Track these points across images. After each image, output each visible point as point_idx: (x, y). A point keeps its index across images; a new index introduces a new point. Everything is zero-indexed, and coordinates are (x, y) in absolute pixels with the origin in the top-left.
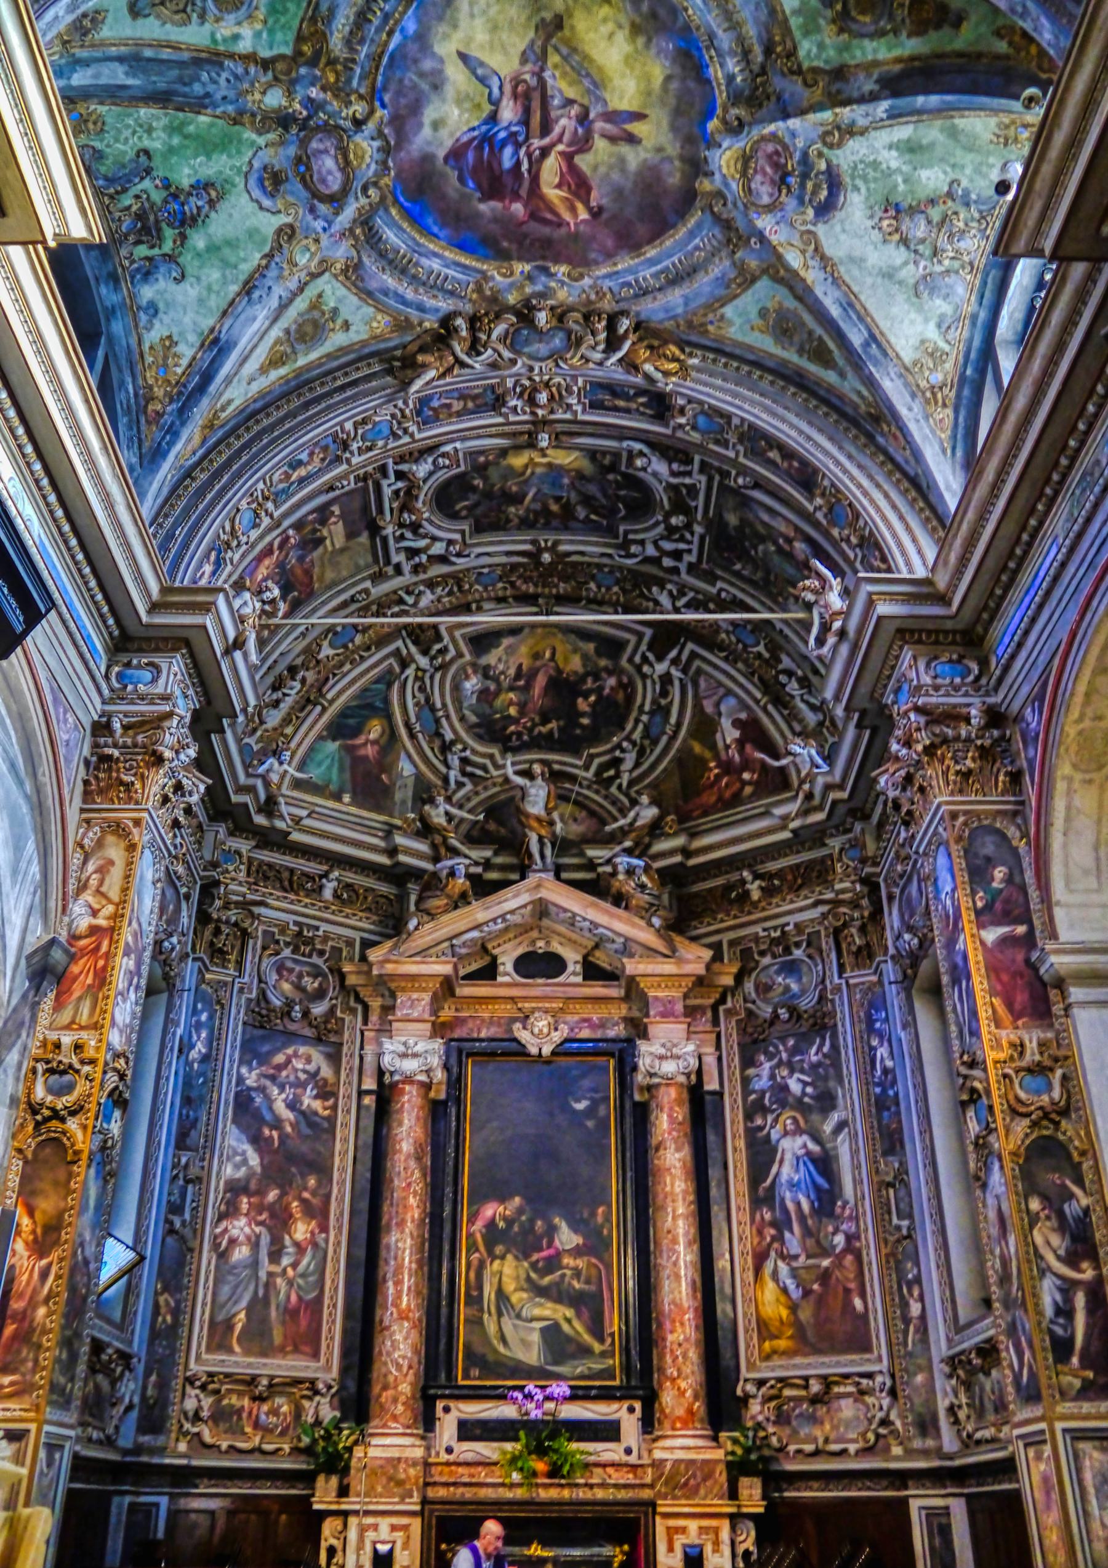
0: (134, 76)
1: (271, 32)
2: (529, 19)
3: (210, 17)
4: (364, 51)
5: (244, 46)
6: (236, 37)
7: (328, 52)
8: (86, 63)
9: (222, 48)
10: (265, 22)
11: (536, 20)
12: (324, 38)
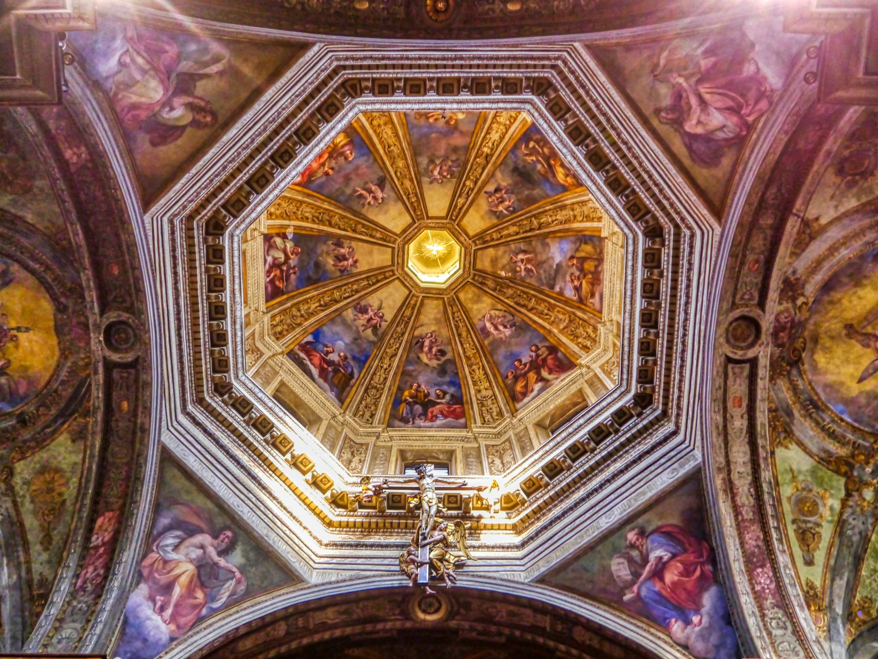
0: (843, 574)
1: (832, 487)
2: (844, 342)
3: (819, 521)
4: (850, 436)
5: (837, 505)
6: (832, 508)
7: (847, 457)
8: (831, 601)
9: (836, 518)
10: (826, 490)
11: (846, 339)
12: (839, 459)
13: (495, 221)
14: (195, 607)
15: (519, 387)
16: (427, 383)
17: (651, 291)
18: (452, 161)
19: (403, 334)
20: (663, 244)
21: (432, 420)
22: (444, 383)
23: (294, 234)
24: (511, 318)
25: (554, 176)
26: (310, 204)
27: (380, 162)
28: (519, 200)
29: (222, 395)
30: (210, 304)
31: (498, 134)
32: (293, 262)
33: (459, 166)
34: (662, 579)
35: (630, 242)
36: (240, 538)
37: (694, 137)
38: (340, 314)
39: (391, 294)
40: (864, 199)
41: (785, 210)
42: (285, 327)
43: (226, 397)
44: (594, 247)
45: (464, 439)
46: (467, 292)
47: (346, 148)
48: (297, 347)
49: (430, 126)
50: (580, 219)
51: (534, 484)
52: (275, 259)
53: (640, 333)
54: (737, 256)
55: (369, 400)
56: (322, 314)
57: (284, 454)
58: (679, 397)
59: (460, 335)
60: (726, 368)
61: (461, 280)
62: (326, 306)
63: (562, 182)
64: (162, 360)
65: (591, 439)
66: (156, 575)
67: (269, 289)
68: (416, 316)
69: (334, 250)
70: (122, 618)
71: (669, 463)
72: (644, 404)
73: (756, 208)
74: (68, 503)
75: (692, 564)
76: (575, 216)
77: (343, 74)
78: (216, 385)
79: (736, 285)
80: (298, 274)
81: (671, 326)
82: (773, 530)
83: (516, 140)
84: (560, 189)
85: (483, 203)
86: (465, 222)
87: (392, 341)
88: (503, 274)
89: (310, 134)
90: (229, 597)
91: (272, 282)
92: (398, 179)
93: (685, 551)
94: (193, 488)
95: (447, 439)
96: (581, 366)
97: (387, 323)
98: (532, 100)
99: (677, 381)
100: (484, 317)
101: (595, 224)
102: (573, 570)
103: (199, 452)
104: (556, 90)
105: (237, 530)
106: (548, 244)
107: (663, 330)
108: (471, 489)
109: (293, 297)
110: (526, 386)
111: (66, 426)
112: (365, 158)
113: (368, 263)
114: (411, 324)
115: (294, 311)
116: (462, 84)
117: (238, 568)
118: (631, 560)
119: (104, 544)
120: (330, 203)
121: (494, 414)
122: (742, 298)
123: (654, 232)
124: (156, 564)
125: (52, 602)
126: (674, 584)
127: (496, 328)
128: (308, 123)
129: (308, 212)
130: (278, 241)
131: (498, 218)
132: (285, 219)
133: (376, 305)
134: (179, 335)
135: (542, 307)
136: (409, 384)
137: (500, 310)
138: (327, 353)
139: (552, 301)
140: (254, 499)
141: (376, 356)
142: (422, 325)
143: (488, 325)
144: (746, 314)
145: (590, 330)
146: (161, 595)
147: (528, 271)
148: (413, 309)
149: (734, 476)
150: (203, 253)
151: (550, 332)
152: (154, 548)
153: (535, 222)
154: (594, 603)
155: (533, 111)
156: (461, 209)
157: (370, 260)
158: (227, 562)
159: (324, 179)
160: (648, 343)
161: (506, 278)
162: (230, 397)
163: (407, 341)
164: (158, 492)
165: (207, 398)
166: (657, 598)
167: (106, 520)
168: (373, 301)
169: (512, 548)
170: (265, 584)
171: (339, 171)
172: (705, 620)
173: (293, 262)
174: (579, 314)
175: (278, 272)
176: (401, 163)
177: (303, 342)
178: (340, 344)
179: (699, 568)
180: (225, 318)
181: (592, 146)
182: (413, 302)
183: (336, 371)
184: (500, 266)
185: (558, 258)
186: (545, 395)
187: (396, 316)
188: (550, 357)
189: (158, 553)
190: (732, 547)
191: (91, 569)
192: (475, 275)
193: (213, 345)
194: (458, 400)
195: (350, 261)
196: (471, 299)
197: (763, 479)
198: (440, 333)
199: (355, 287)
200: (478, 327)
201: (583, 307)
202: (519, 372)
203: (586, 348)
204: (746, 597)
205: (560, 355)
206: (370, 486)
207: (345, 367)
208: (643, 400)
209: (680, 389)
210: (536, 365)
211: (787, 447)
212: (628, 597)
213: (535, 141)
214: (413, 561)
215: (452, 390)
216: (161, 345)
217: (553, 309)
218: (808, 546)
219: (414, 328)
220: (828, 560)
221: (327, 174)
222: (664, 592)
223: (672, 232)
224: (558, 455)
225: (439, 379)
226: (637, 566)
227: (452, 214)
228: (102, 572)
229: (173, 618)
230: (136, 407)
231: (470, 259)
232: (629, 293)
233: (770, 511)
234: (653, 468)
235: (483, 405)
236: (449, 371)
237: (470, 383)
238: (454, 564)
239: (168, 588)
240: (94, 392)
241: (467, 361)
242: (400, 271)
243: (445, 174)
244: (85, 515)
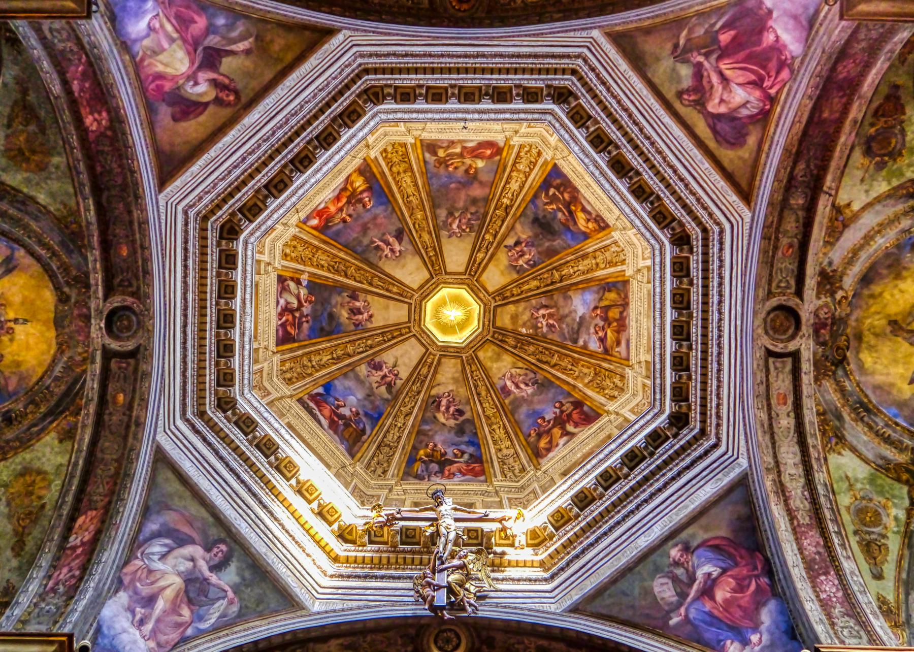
1: (894, 496)
2: (890, 340)
3: (884, 532)
5: (902, 515)
6: (896, 519)
7: (907, 464)
9: (902, 529)
10: (888, 499)
11: (891, 336)
12: (898, 465)
13: (515, 276)
14: (178, 625)
15: (543, 444)
16: (444, 442)
17: (681, 301)
18: (471, 214)
19: (419, 393)
20: (691, 251)
21: (448, 477)
22: (462, 443)
24: (532, 375)
25: (575, 223)
26: (326, 251)
27: (399, 213)
28: (539, 253)
29: (224, 411)
30: (219, 311)
31: (518, 184)
32: (306, 309)
33: (478, 219)
34: (712, 598)
35: (657, 253)
36: (236, 554)
37: (718, 117)
39: (406, 352)
40: (895, 183)
41: (815, 188)
42: (295, 375)
43: (229, 413)
44: (619, 294)
45: (484, 493)
46: (487, 351)
47: (365, 195)
48: (306, 396)
49: (450, 176)
50: (603, 266)
51: (563, 517)
52: (288, 303)
53: (671, 346)
54: (770, 239)
55: (381, 457)
56: (334, 367)
57: (288, 480)
58: (718, 405)
59: (479, 394)
60: (767, 362)
61: (480, 338)
63: (583, 229)
64: (164, 352)
65: (623, 464)
66: (138, 585)
67: (280, 333)
68: (433, 375)
69: (349, 302)
70: (95, 625)
71: (712, 475)
72: (680, 425)
73: (786, 186)
74: (48, 507)
75: (744, 579)
76: (597, 264)
77: (366, 80)
78: (219, 399)
79: (771, 271)
80: (311, 323)
81: (705, 336)
82: (833, 535)
83: (535, 189)
84: (582, 238)
85: (503, 258)
86: (484, 277)
87: (406, 400)
88: (524, 331)
89: (330, 139)
90: (220, 617)
91: (283, 325)
92: (417, 231)
93: (737, 564)
94: (188, 494)
95: (466, 492)
96: (608, 412)
98: (553, 110)
99: (714, 387)
100: (504, 376)
101: (619, 268)
102: (610, 595)
103: (197, 459)
104: (577, 98)
105: (233, 544)
107: (697, 341)
108: (493, 520)
109: (305, 346)
110: (550, 442)
111: (54, 425)
114: (427, 382)
115: (305, 361)
116: (483, 92)
117: (231, 588)
118: (675, 579)
119: (83, 544)
120: (347, 253)
121: (517, 471)
122: (778, 287)
123: (681, 240)
124: (139, 572)
125: (17, 603)
126: (726, 601)
127: (517, 387)
128: (330, 129)
129: (323, 259)
130: (292, 285)
131: (518, 272)
134: (184, 333)
135: (565, 363)
136: (424, 444)
138: (338, 407)
139: (576, 355)
140: (253, 516)
141: (389, 414)
143: (509, 383)
144: (784, 303)
145: (617, 380)
146: (143, 607)
147: (550, 326)
148: (430, 367)
149: (786, 479)
150: (216, 257)
151: (574, 387)
152: (139, 555)
153: (557, 275)
154: (636, 631)
155: (554, 121)
156: (480, 264)
158: (220, 579)
160: (681, 358)
161: (527, 335)
162: (234, 414)
163: (423, 400)
164: (148, 495)
165: (209, 412)
166: (708, 619)
167: (88, 520)
168: (388, 358)
169: (540, 581)
170: (261, 608)
171: (356, 220)
172: (765, 638)
173: (306, 309)
175: (290, 317)
176: (419, 215)
178: (352, 399)
179: (754, 583)
180: (235, 269)
181: (615, 153)
182: (429, 360)
183: (347, 425)
184: (520, 322)
186: (571, 445)
187: (411, 375)
188: (575, 412)
189: (143, 560)
190: (790, 553)
191: (65, 570)
192: (494, 333)
193: (219, 356)
194: (477, 459)
195: (365, 315)
196: (490, 358)
197: (817, 481)
199: (369, 342)
200: (498, 386)
201: (609, 358)
202: (542, 429)
203: (623, 262)
204: (811, 604)
205: (585, 408)
206: (383, 514)
207: (357, 422)
208: (679, 420)
209: (718, 396)
210: (560, 421)
211: (839, 453)
212: (674, 621)
213: (555, 188)
214: (429, 584)
215: (471, 450)
216: (165, 336)
217: (577, 363)
218: (875, 558)
219: (431, 387)
220: (899, 573)
221: (344, 221)
222: (716, 613)
223: (700, 237)
224: (588, 483)
225: (457, 439)
226: (682, 586)
228: (77, 573)
229: (154, 632)
230: (133, 399)
231: (490, 314)
232: (658, 306)
233: (828, 514)
234: (694, 482)
235: (504, 464)
236: (467, 431)
237: (490, 442)
238: (475, 594)
239: (150, 601)
240: (89, 384)
241: (486, 420)
242: (417, 328)
243: (464, 227)
244: (65, 513)
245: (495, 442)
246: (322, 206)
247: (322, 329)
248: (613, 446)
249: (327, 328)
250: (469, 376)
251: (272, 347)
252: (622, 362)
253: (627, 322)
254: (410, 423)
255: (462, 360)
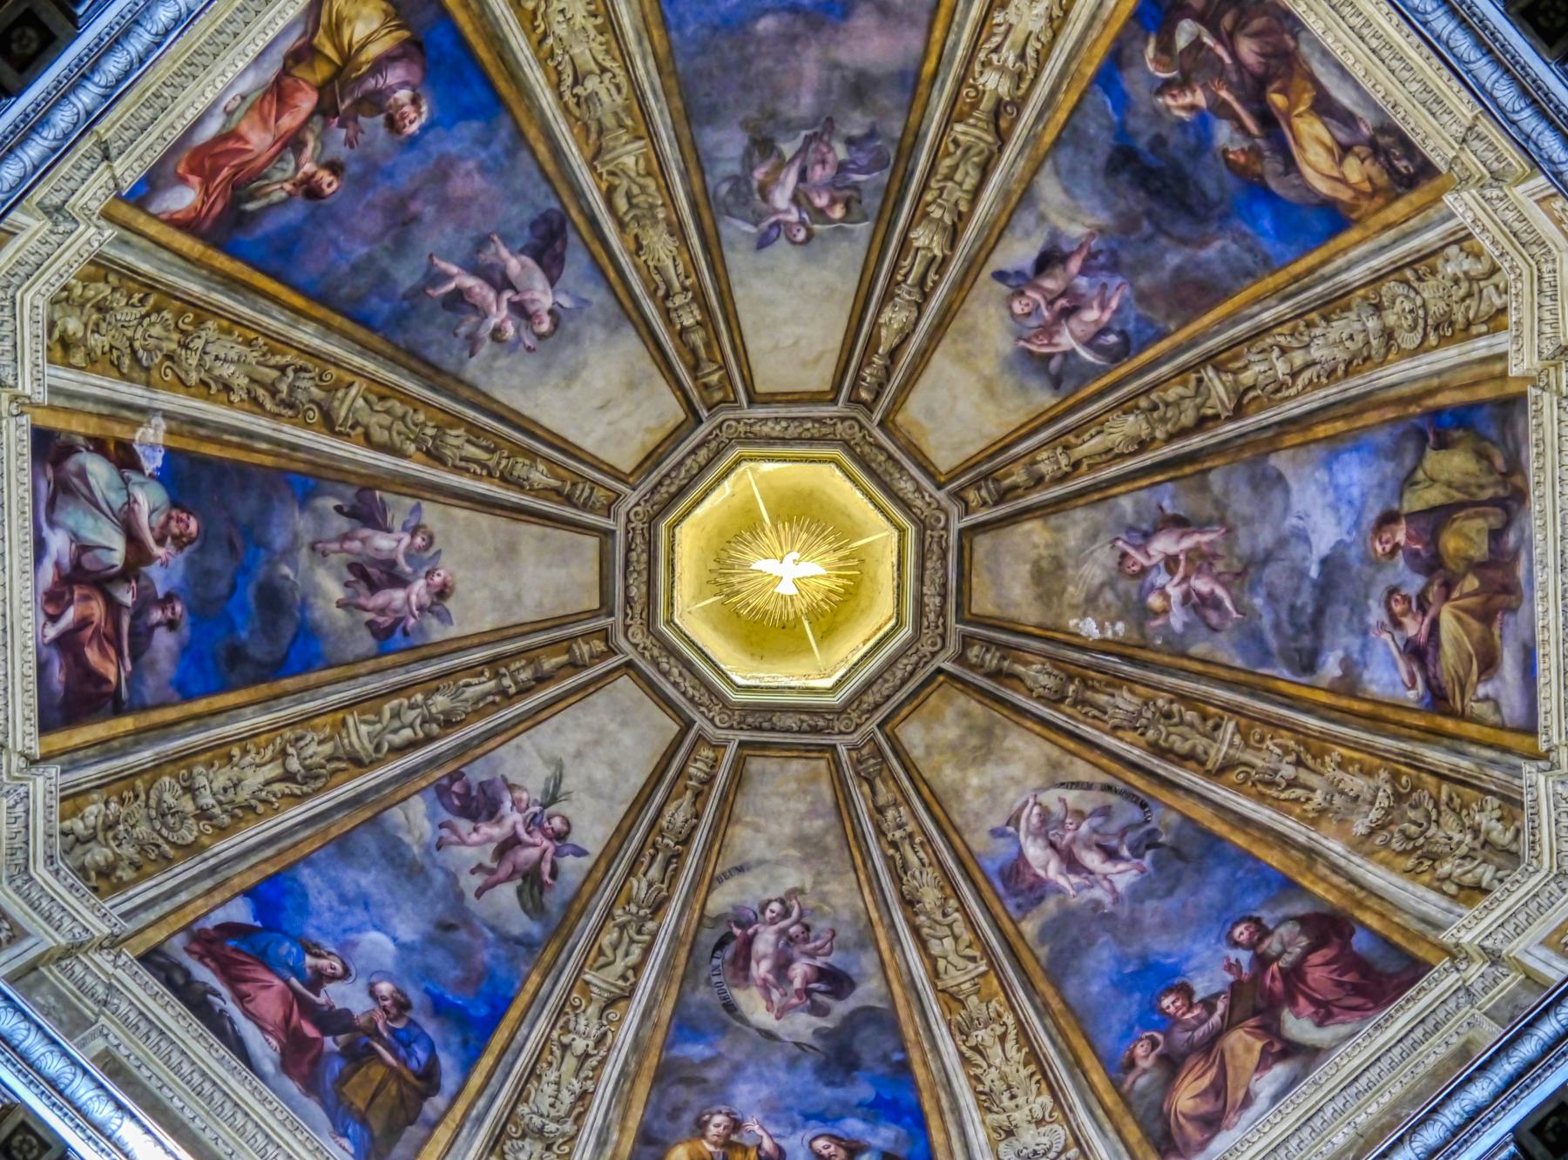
15: (1187, 1097)
16: (774, 1111)
18: (850, 142)
19: (658, 907)
22: (847, 1110)
23: (170, 453)
24: (1135, 814)
25: (1290, 164)
27: (542, 150)
28: (1142, 297)
33: (878, 163)
38: (373, 821)
42: (128, 851)
44: (1481, 455)
46: (937, 716)
47: (395, 75)
48: (179, 942)
50: (1409, 340)
52: (83, 548)
56: (295, 814)
59: (910, 903)
61: (906, 664)
62: (311, 778)
63: (1323, 187)
67: (57, 675)
68: (714, 829)
69: (345, 537)
80: (185, 630)
83: (1115, 27)
84: (1319, 225)
86: (915, 408)
87: (607, 939)
88: (1089, 628)
91: (68, 644)
92: (622, 225)
96: (1454, 954)
97: (587, 862)
100: (1014, 820)
101: (1480, 347)
106: (1280, 477)
109: (166, 729)
110: (1218, 1089)
112: (476, 125)
113: (497, 598)
114: (691, 861)
115: (168, 790)
127: (1072, 863)
130: (99, 471)
131: (1056, 382)
132: (124, 377)
133: (534, 783)
135: (1268, 756)
137: (1089, 786)
138: (318, 980)
142: (740, 869)
143: (1035, 852)
145: (1487, 819)
147: (1199, 604)
151: (1311, 854)
153: (1219, 387)
156: (893, 354)
157: (507, 588)
159: (296, 212)
163: (675, 939)
171: (362, 183)
174: (1436, 756)
175: (97, 609)
177: (210, 924)
178: (377, 945)
182: (697, 769)
183: (358, 1055)
184: (1075, 593)
185: (1326, 533)
186: (1306, 1097)
187: (622, 833)
188: (1316, 958)
192: (966, 641)
196: (954, 748)
198: (824, 898)
199: (440, 702)
200: (991, 867)
201: (1449, 725)
202: (1181, 1037)
205: (1360, 942)
213: (1200, 18)
217: (1319, 755)
219: (706, 882)
221: (310, 190)
225: (827, 1092)
227: (858, 377)
236: (868, 1056)
237: (967, 1099)
243: (821, 201)
245: (986, 1101)
246: (212, 128)
247: (236, 655)
248: (1480, 1092)
249: (258, 650)
250: (869, 828)
251: (25, 735)
252: (1509, 739)
253: (1521, 572)
254: (625, 1036)
255: (837, 762)
